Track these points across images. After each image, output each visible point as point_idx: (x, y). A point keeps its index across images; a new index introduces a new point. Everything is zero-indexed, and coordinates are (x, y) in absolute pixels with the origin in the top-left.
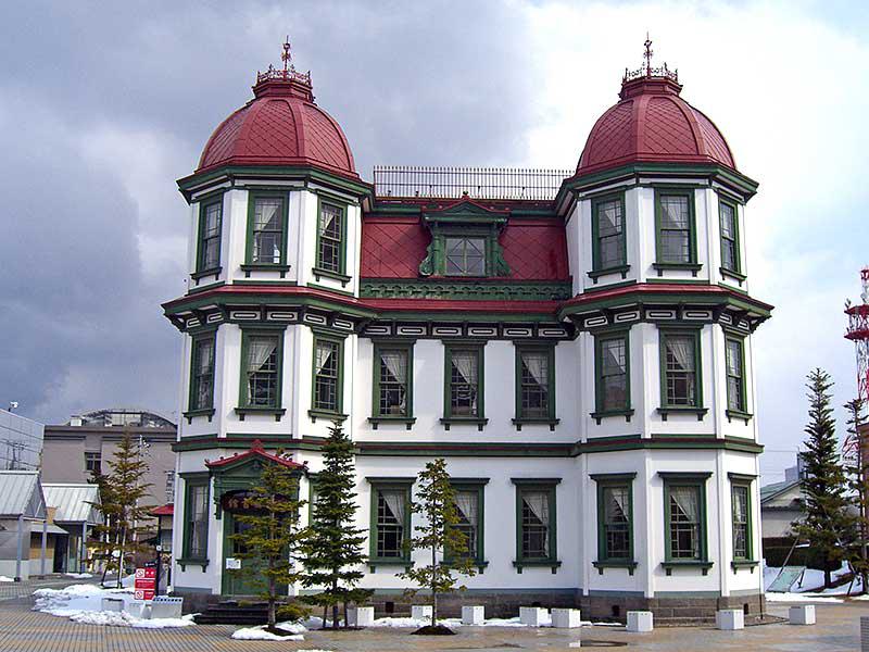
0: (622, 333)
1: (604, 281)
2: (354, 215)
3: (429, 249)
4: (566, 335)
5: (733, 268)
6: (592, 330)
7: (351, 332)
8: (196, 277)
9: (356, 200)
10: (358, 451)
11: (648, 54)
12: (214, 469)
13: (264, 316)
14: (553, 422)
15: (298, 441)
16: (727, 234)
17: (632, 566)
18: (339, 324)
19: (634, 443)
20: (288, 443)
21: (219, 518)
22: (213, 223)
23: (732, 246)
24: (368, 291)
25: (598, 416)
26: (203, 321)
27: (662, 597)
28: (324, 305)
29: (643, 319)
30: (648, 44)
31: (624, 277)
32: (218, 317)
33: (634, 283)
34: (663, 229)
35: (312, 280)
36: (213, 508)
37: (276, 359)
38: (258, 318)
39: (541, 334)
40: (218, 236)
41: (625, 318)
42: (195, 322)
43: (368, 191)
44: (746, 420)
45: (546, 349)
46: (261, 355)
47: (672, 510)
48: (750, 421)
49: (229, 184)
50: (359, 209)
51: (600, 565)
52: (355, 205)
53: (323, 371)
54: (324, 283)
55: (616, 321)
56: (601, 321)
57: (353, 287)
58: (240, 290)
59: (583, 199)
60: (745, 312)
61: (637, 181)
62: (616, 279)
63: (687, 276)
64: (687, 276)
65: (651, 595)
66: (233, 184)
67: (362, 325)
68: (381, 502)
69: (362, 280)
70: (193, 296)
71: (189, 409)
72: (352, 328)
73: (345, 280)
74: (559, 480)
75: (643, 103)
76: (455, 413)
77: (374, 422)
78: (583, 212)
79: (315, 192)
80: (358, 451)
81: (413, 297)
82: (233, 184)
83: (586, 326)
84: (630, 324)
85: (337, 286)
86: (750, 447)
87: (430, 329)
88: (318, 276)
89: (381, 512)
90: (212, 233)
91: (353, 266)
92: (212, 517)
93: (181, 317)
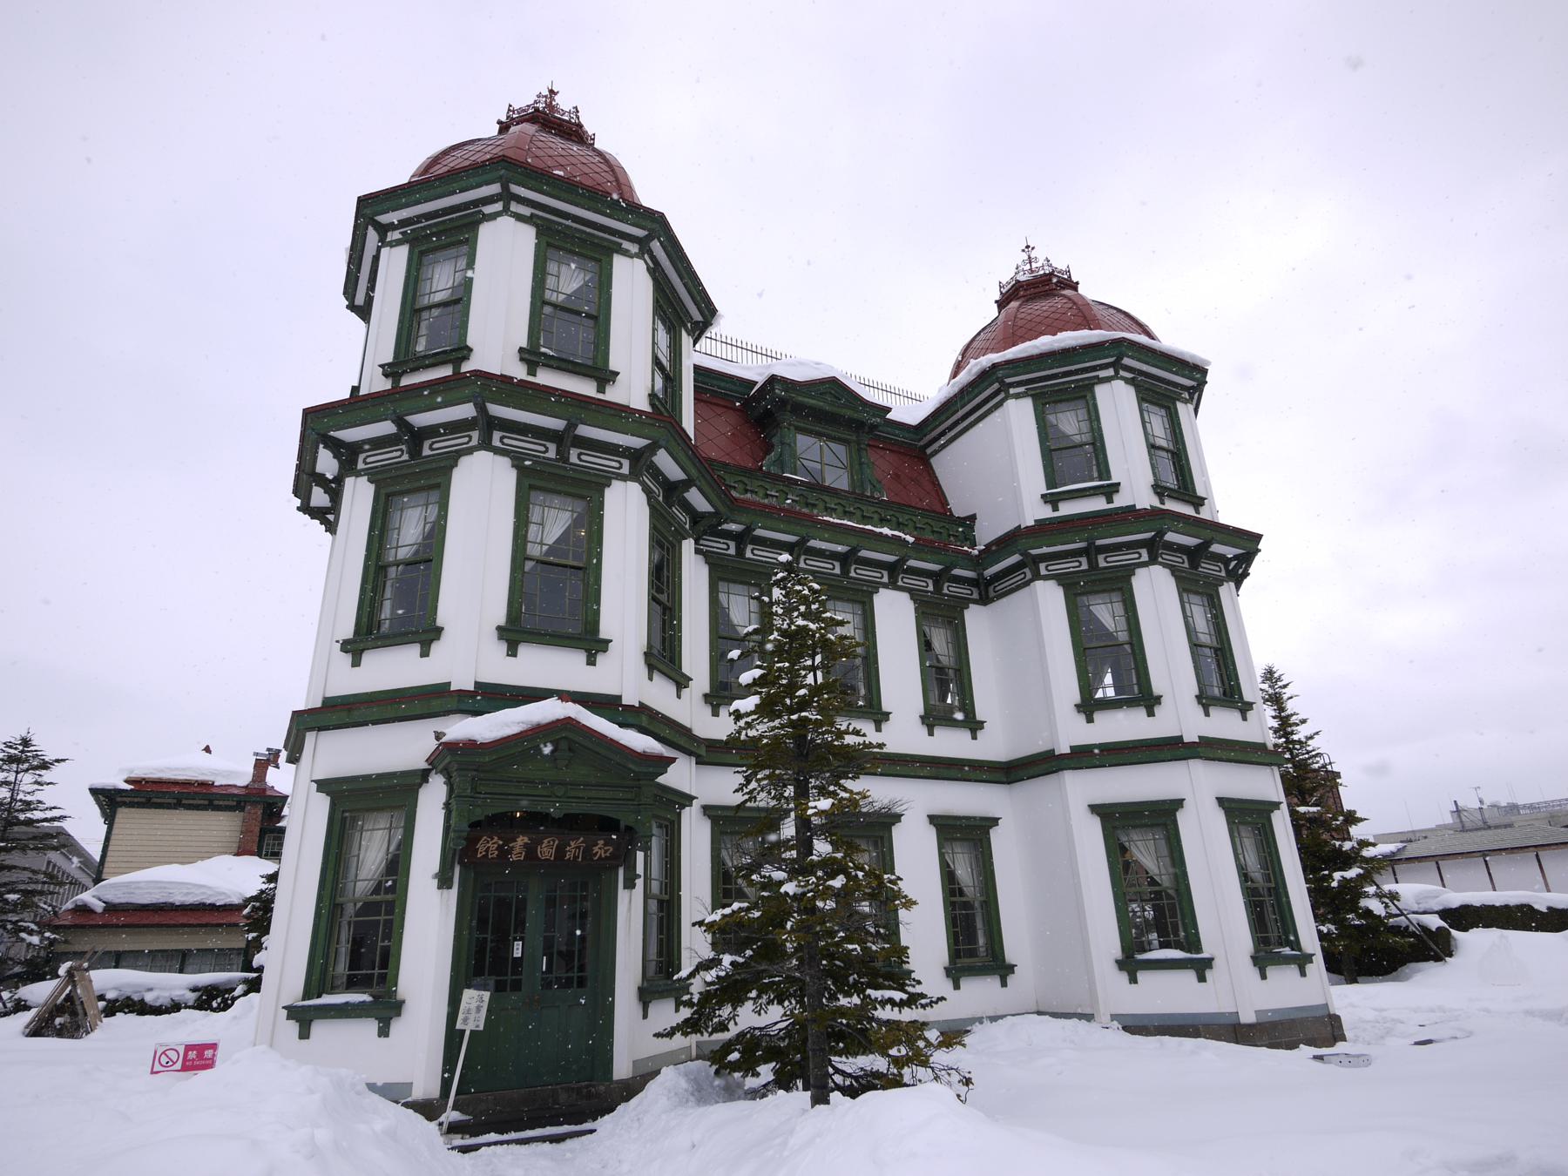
0: (1119, 584)
1: (1068, 509)
6: (1063, 580)
14: (974, 726)
19: (1170, 749)
21: (444, 881)
26: (415, 452)
27: (1270, 1017)
46: (554, 523)
61: (1117, 373)
71: (357, 632)
74: (994, 821)
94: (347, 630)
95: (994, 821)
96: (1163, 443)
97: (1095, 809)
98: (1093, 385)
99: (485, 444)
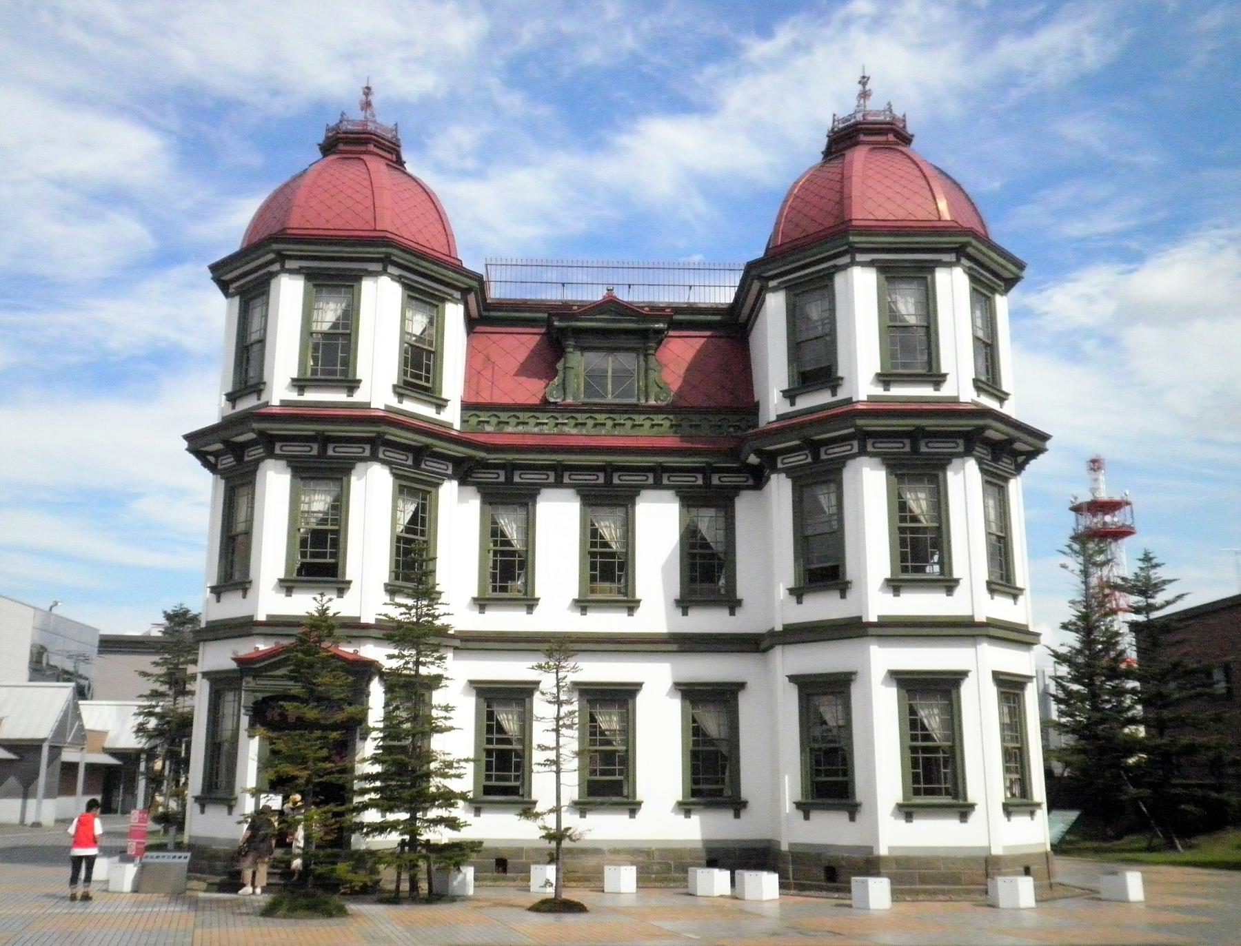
1: (804, 402)
2: (454, 314)
3: (560, 366)
4: (751, 482)
5: (989, 381)
6: (790, 472)
7: (450, 478)
8: (232, 398)
9: (457, 295)
10: (457, 643)
11: (864, 95)
12: (247, 666)
13: (323, 449)
14: (733, 604)
15: (367, 626)
16: (980, 334)
17: (852, 810)
18: (429, 465)
20: (355, 629)
22: (255, 324)
23: (987, 349)
24: (474, 421)
25: (798, 593)
26: (239, 459)
28: (410, 435)
29: (863, 452)
30: (864, 81)
31: (834, 394)
32: (258, 451)
33: (849, 401)
34: (892, 327)
35: (393, 402)
36: (245, 721)
37: (339, 507)
38: (315, 452)
39: (715, 480)
40: (262, 341)
41: (838, 451)
42: (228, 461)
43: (474, 284)
44: (1015, 597)
45: (723, 501)
47: (913, 726)
48: (1021, 598)
49: (276, 267)
50: (461, 308)
51: (805, 808)
52: (455, 301)
53: (408, 530)
54: (410, 406)
55: (824, 457)
56: (802, 458)
57: (452, 416)
58: (291, 415)
59: (775, 289)
60: (1011, 441)
62: (822, 398)
63: (926, 391)
64: (926, 391)
65: (883, 851)
66: (283, 266)
67: (465, 467)
68: (490, 716)
69: (467, 407)
70: (228, 424)
72: (450, 472)
73: (441, 405)
74: (741, 686)
75: (859, 157)
76: (593, 591)
77: (481, 603)
78: (775, 304)
79: (399, 279)
80: (457, 643)
81: (536, 430)
82: (283, 266)
83: (780, 465)
84: (841, 462)
85: (427, 411)
86: (1019, 637)
87: (559, 476)
88: (401, 396)
89: (490, 727)
90: (254, 337)
91: (453, 382)
92: (243, 734)
93: (211, 453)
94: (214, 582)
95: (741, 686)
96: (912, 320)
97: (793, 679)
98: (833, 273)
99: (271, 454)
